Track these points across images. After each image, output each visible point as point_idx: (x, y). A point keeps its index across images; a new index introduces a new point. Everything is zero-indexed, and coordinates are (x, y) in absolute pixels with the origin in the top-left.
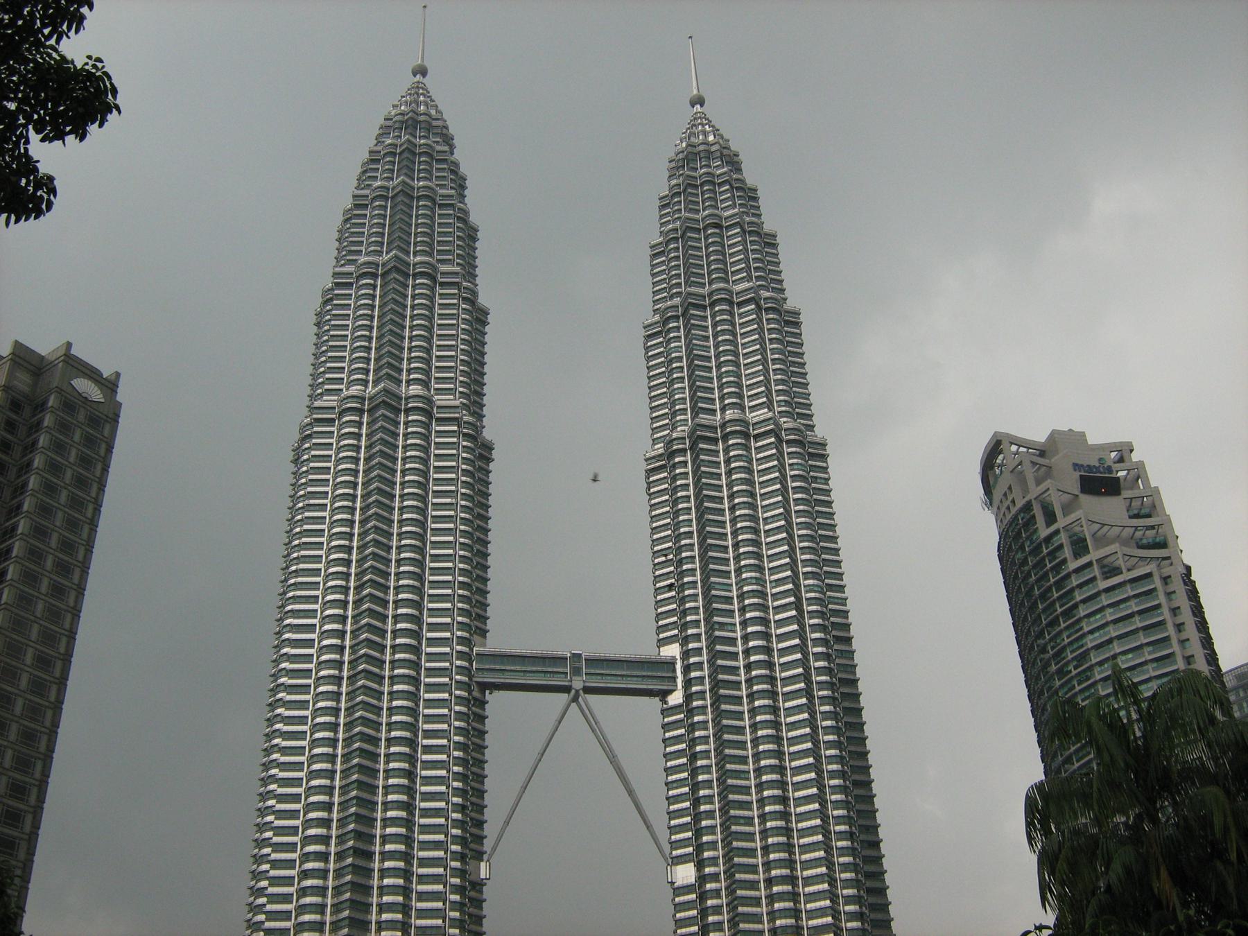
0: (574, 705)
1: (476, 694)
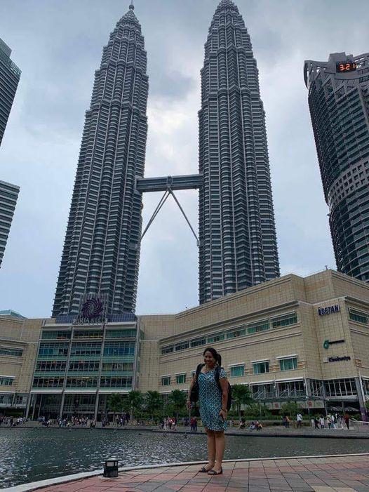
0: (171, 194)
1: (136, 192)
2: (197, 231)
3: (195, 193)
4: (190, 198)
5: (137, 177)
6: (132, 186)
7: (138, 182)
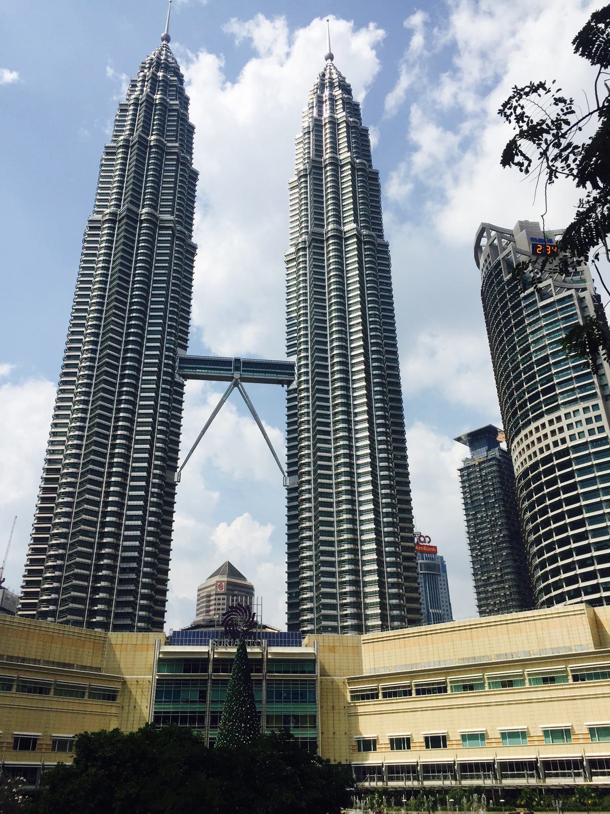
0: (236, 388)
2: (284, 460)
5: (180, 352)
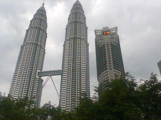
3: (60, 76)
4: (57, 78)
6: (35, 75)
7: (38, 73)
